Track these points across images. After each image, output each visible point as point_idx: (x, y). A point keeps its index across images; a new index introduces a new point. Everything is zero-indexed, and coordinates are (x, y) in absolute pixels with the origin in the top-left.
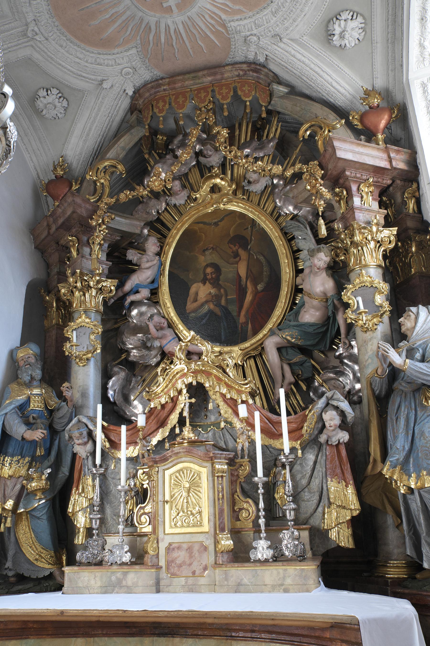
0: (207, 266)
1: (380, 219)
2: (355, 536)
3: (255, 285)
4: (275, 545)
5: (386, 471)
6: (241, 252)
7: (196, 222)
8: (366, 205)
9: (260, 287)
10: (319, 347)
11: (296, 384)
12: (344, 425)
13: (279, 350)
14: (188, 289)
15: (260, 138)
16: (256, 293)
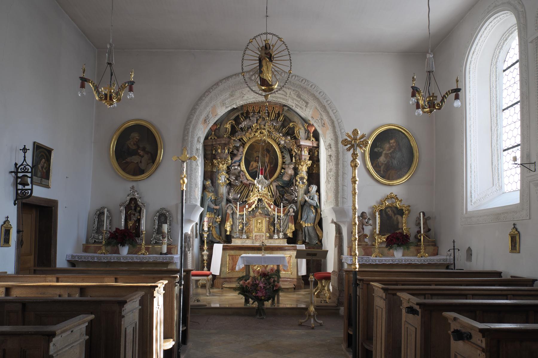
1: (308, 158)
2: (293, 235)
3: (271, 165)
4: (278, 236)
7: (254, 142)
8: (305, 154)
9: (272, 166)
11: (280, 196)
12: (293, 212)
15: (277, 120)
16: (271, 167)
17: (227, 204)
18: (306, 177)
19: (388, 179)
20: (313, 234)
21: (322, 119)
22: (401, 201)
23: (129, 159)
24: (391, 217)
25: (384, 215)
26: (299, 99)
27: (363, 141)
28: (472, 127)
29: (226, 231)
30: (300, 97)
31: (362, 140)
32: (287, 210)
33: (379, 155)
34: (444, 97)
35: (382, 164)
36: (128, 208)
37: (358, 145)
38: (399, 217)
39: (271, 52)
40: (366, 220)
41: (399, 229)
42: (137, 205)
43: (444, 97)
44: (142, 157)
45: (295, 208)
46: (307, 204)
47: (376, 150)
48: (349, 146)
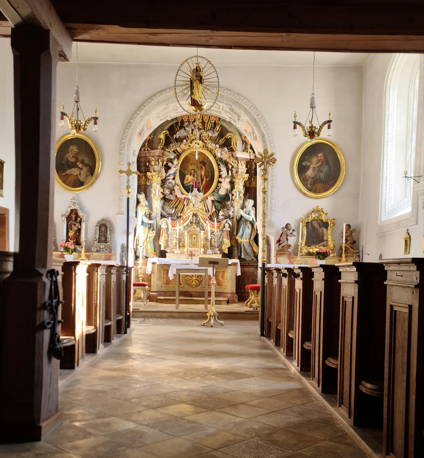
0: (192, 170)
2: (229, 251)
3: (206, 178)
5: (237, 238)
6: (203, 167)
8: (242, 168)
9: (208, 179)
10: (223, 202)
11: (216, 211)
12: (229, 227)
13: (212, 201)
14: (185, 176)
15: (214, 130)
16: (206, 181)
17: (161, 218)
18: (243, 192)
19: (315, 192)
20: (249, 250)
21: (254, 133)
22: (326, 214)
23: (68, 172)
24: (317, 230)
25: (310, 227)
26: (232, 113)
27: (272, 159)
28: (389, 142)
29: (160, 246)
30: (232, 110)
31: (271, 158)
32: (222, 225)
33: (307, 168)
34: (321, 127)
35: (310, 177)
36: (69, 219)
37: (268, 162)
38: (325, 230)
39: (201, 75)
41: (324, 241)
42: (77, 216)
43: (321, 127)
44: (81, 169)
45: (230, 223)
46: (243, 219)
47: (304, 164)
48: (260, 163)
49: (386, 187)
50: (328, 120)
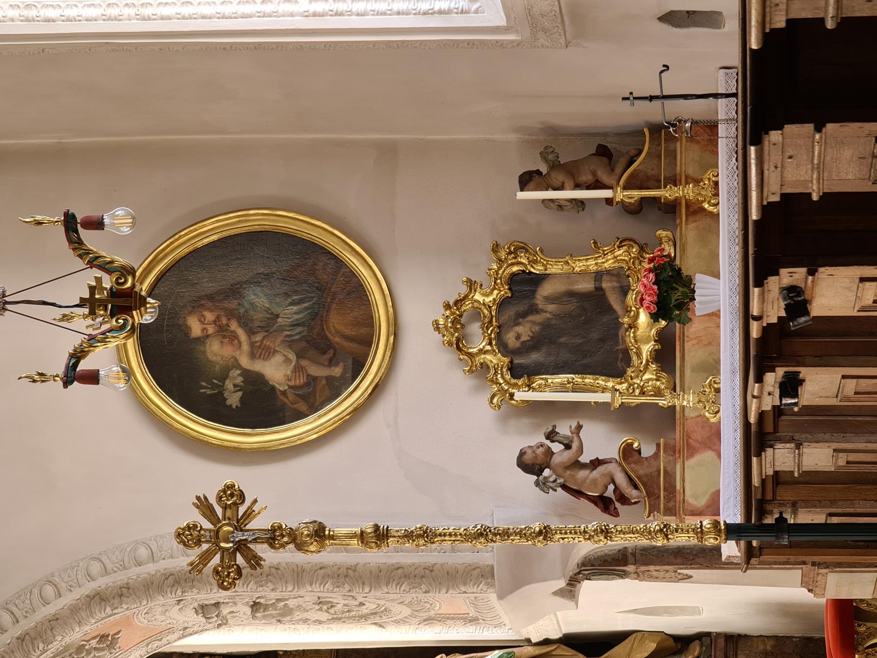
19: (367, 342)
22: (471, 285)
24: (546, 326)
25: (535, 357)
27: (225, 508)
28: (147, 12)
31: (219, 511)
33: (255, 384)
34: (94, 262)
35: (298, 369)
37: (240, 524)
38: (546, 289)
40: (556, 447)
41: (599, 289)
43: (94, 262)
47: (234, 399)
48: (240, 560)
49: (350, 13)
50: (62, 229)
